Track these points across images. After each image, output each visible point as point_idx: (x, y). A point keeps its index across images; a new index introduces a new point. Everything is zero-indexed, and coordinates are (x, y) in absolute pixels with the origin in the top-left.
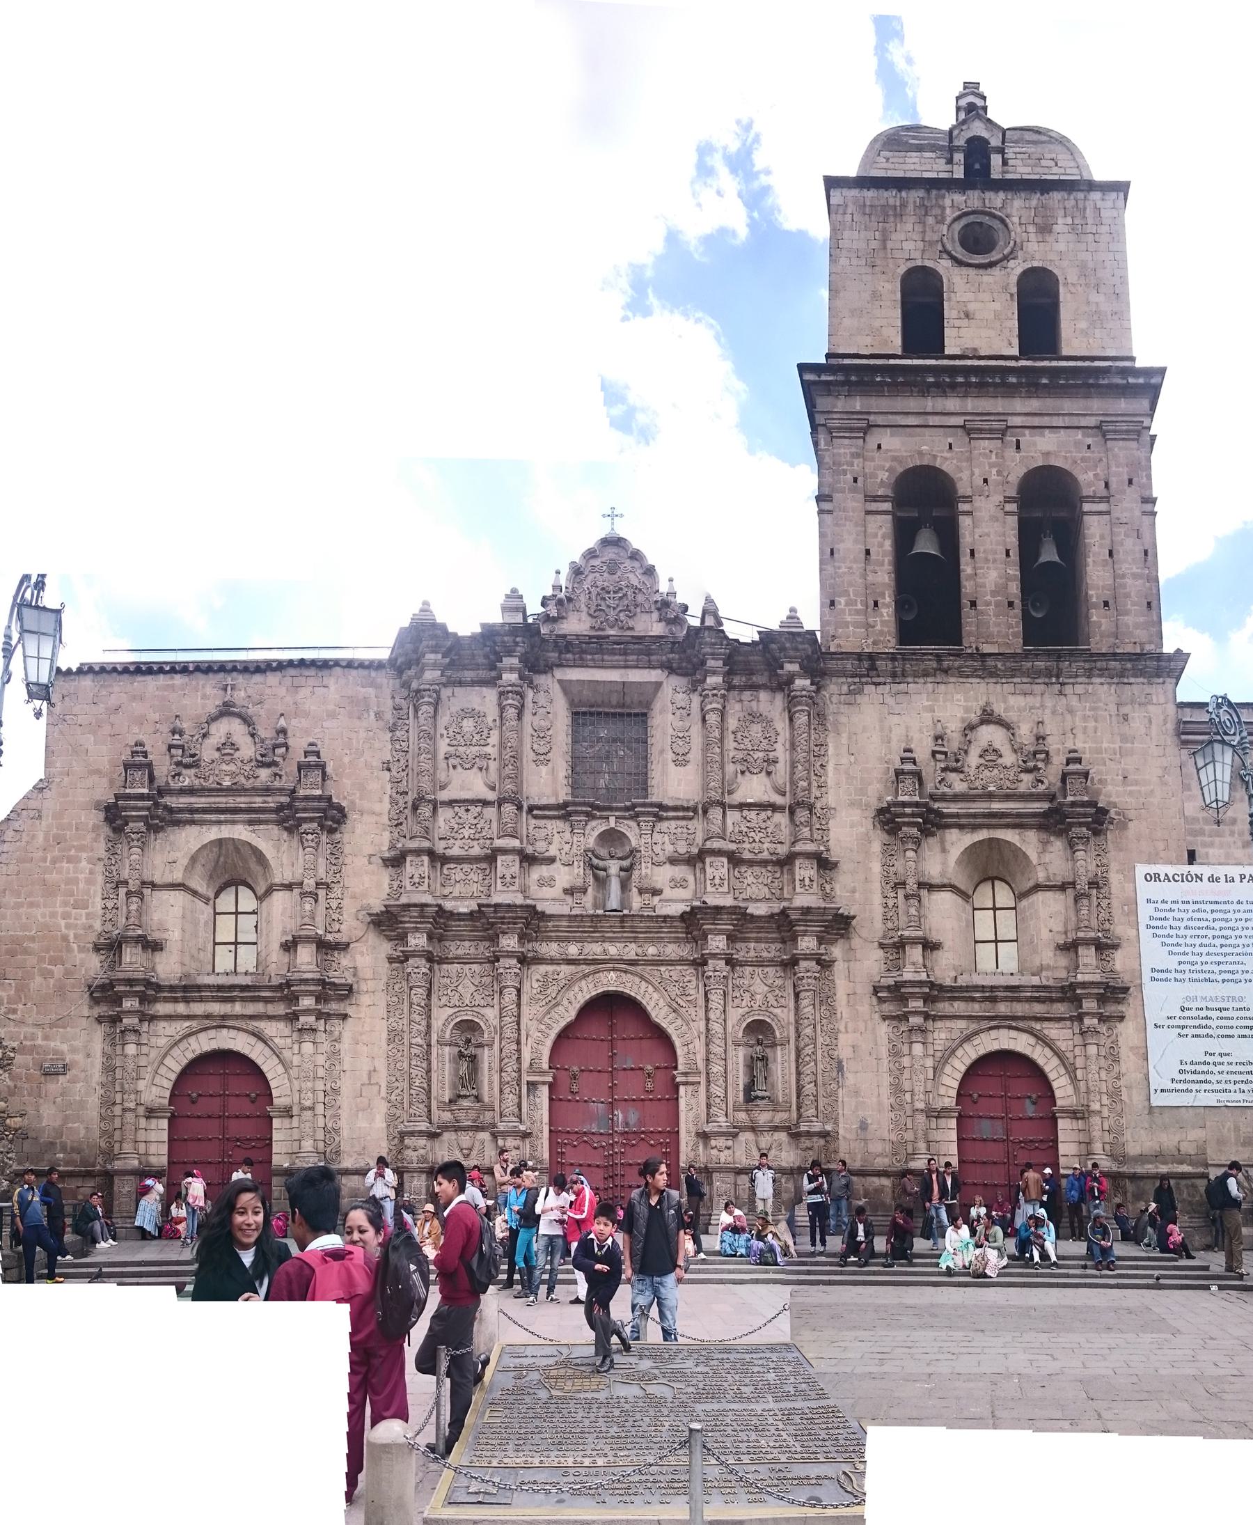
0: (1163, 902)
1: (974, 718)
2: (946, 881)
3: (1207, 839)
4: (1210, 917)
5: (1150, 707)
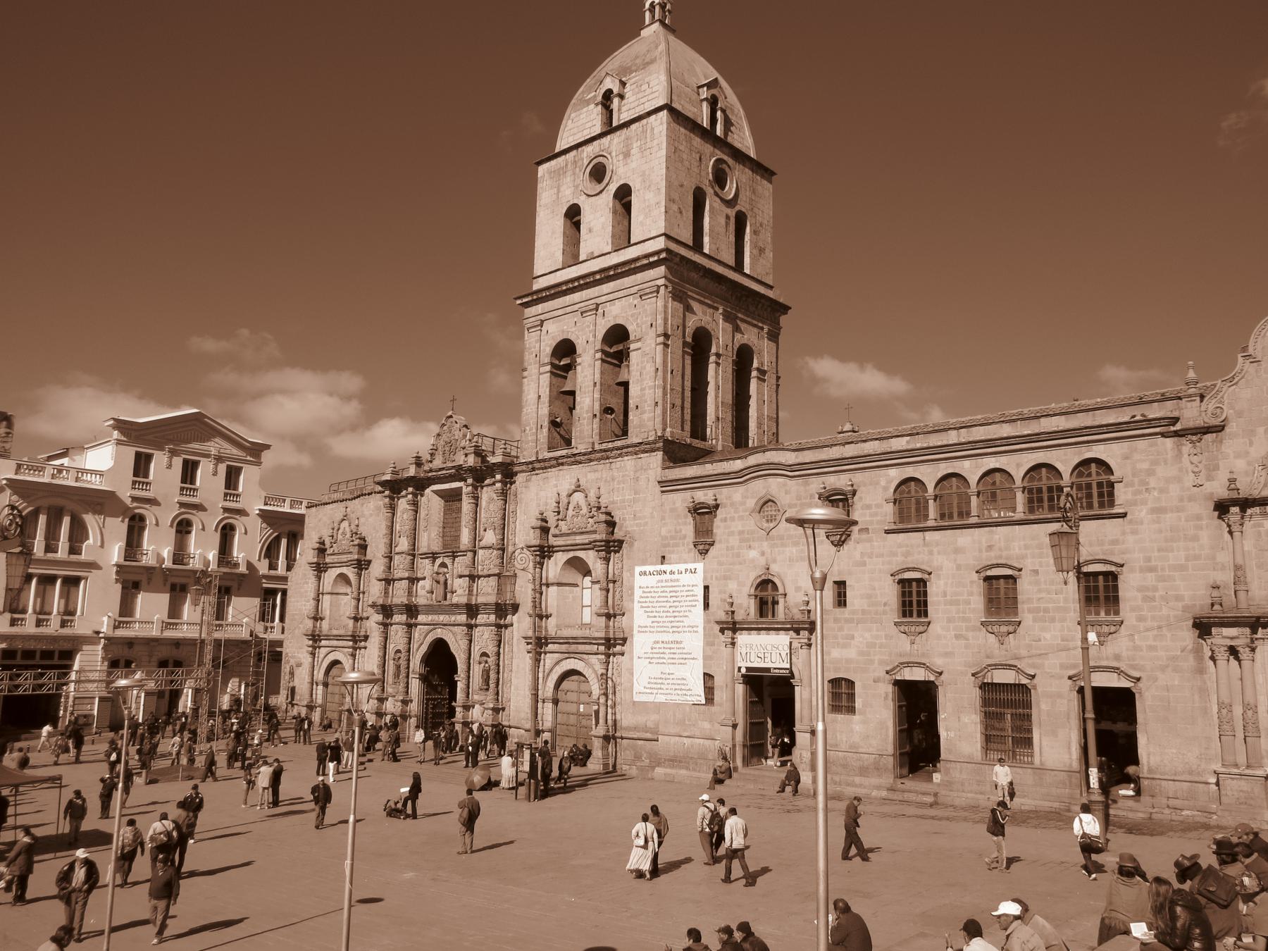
0: (647, 587)
1: (573, 487)
2: (556, 581)
3: (671, 549)
4: (669, 595)
5: (650, 471)
